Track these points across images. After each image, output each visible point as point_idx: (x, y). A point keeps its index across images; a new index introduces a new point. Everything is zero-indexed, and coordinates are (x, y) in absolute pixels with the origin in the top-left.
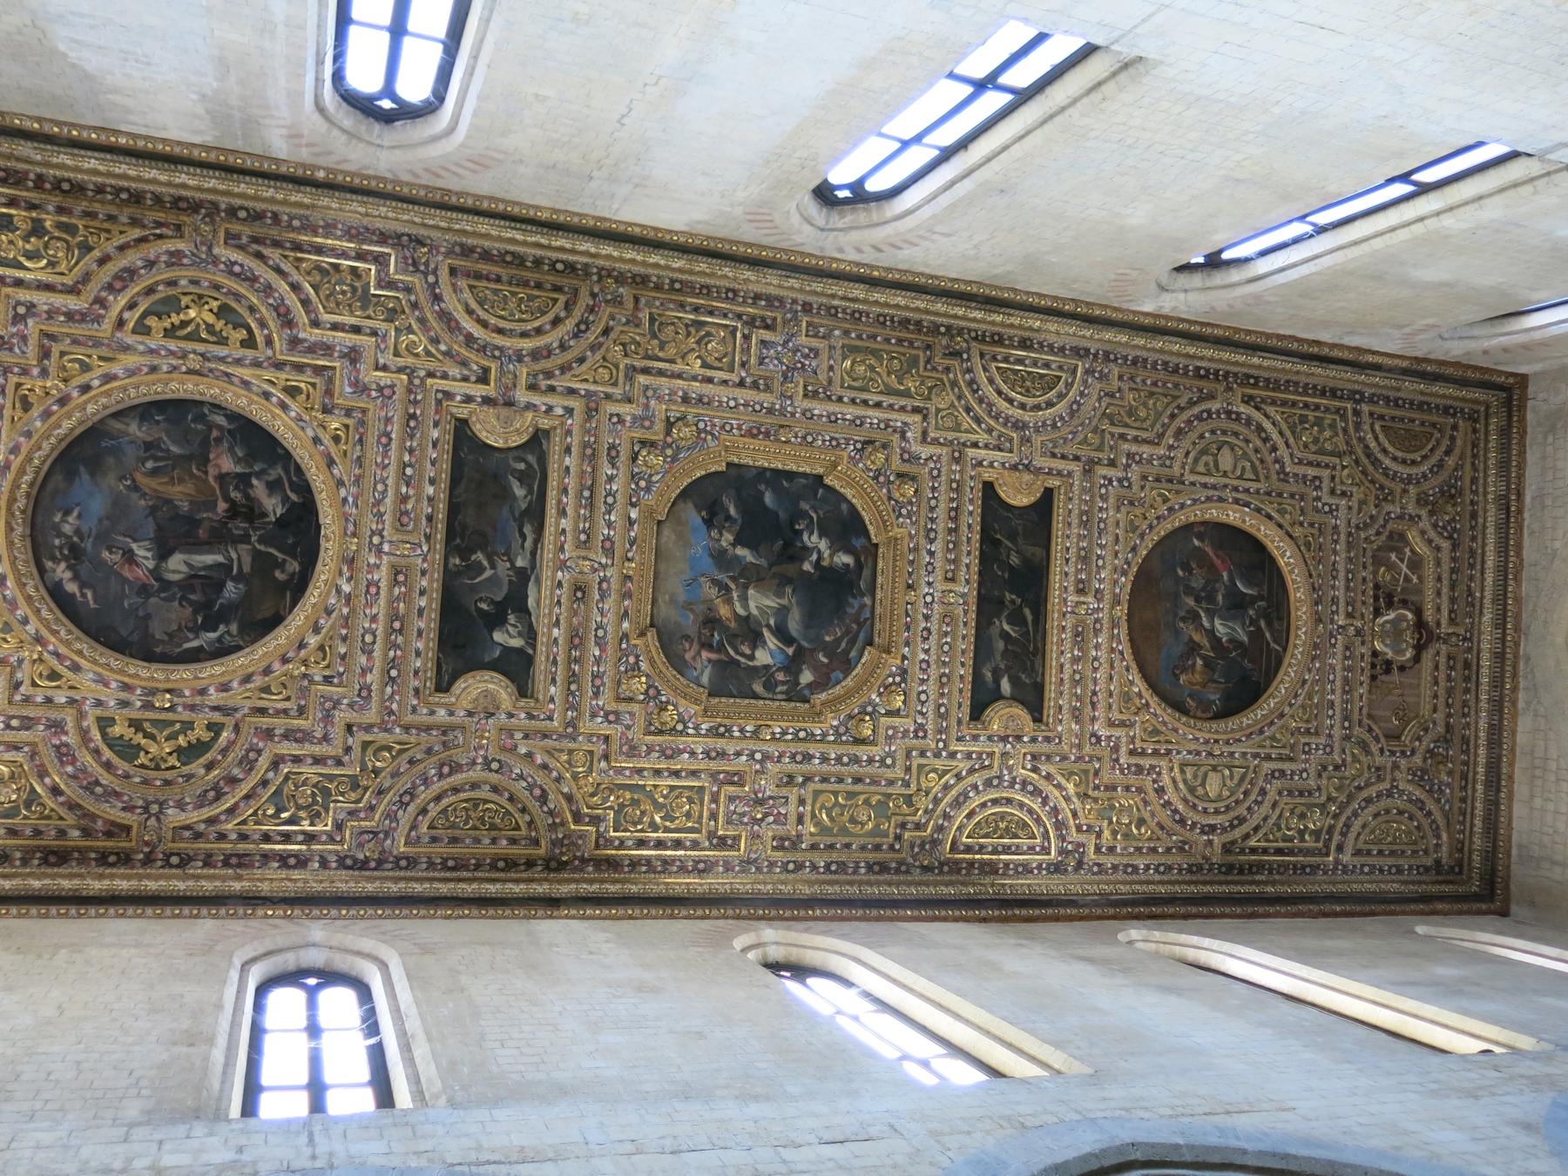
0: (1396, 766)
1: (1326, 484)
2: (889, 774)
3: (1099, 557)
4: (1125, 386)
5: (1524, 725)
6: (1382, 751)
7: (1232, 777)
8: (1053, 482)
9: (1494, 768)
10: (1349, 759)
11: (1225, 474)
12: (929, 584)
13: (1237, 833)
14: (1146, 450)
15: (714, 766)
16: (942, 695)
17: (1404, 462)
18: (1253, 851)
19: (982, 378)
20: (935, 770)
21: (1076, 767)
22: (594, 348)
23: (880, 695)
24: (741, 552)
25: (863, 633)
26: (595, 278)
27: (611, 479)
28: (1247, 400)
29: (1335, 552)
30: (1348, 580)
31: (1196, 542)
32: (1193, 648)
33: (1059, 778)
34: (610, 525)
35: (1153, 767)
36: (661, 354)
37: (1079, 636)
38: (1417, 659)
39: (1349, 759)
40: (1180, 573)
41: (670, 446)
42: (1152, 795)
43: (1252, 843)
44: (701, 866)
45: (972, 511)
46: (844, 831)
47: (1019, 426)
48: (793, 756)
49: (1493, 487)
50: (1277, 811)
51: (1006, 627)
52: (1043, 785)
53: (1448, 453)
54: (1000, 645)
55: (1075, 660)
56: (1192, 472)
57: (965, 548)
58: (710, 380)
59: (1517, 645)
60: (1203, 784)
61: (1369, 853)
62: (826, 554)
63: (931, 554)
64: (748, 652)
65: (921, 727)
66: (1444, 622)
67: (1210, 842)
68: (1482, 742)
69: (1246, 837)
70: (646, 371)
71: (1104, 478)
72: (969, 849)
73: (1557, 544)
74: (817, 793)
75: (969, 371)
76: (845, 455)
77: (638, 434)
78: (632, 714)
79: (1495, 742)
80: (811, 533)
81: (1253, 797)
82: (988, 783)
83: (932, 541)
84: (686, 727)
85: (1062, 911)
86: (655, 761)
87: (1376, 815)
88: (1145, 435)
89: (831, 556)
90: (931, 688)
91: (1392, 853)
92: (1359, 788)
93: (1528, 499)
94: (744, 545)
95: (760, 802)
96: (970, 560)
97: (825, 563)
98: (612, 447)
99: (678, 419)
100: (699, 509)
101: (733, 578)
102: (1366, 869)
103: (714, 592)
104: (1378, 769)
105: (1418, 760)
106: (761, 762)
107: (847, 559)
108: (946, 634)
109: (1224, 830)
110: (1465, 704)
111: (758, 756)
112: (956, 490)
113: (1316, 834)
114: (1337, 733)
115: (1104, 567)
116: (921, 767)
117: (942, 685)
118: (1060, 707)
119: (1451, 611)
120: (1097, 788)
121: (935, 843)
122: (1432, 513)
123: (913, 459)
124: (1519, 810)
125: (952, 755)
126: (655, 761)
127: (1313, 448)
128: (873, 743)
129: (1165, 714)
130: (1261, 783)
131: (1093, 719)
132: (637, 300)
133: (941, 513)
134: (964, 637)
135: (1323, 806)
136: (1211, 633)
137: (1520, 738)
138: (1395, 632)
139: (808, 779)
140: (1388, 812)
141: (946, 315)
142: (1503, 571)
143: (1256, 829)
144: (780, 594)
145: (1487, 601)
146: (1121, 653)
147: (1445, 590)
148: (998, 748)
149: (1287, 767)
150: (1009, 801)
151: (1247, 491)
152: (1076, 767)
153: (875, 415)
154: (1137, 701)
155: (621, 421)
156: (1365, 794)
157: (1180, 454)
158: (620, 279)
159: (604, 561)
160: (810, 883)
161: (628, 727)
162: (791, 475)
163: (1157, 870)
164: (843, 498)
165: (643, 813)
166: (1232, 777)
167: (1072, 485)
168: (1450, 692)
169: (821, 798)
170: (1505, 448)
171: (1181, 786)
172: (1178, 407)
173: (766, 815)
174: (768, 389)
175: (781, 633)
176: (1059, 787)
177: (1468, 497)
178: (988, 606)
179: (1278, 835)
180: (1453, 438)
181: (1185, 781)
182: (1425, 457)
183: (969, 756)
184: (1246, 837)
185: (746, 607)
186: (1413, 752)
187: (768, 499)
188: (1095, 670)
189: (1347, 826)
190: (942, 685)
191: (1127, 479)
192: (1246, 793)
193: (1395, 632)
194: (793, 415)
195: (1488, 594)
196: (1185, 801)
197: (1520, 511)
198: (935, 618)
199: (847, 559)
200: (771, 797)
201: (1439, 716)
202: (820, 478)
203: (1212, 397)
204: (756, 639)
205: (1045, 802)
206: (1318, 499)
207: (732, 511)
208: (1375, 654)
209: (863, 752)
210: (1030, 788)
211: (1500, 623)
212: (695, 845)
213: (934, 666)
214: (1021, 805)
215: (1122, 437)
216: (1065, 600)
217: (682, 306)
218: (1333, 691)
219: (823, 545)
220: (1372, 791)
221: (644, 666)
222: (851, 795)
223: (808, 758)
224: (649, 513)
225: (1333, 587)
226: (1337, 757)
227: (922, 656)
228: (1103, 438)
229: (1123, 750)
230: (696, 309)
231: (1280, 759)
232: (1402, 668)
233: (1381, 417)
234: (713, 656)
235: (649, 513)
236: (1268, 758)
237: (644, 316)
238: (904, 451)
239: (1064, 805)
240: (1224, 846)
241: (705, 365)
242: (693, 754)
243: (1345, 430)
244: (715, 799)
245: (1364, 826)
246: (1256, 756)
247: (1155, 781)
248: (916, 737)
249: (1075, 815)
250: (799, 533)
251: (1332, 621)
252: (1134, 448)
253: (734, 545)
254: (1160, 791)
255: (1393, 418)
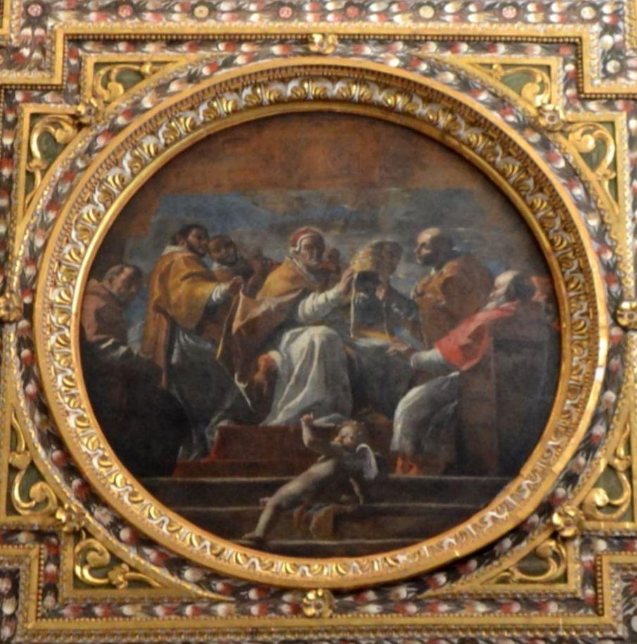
32: (249, 273)
40: (426, 236)
136: (287, 319)
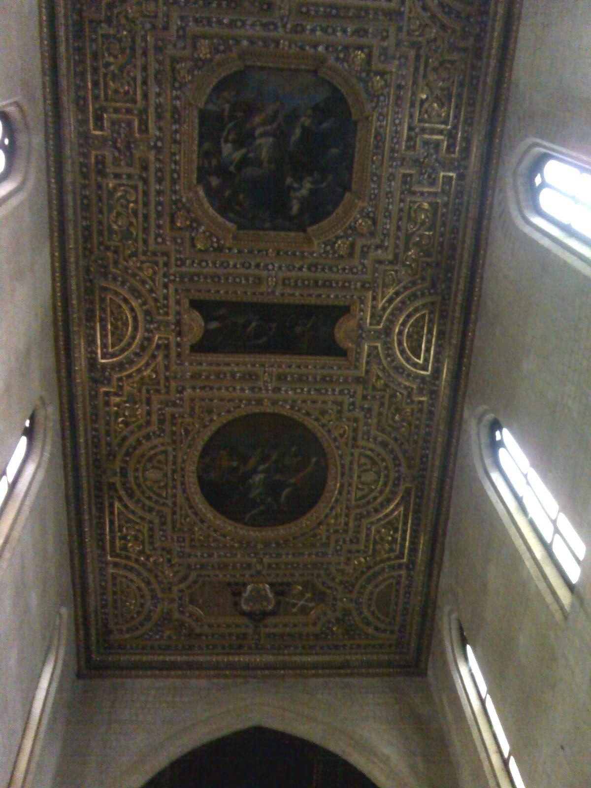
0: (172, 601)
1: (354, 547)
2: (151, 241)
3: (302, 390)
4: (415, 407)
5: (204, 683)
6: (181, 591)
7: (160, 488)
8: (352, 356)
9: (174, 666)
10: (175, 569)
11: (359, 477)
12: (280, 268)
13: (122, 493)
14: (373, 421)
15: (151, 110)
16: (206, 278)
17: (370, 599)
18: (111, 505)
19: (418, 303)
20: (155, 273)
21: (162, 377)
22: (433, 16)
23: (204, 232)
24: (298, 131)
25: (247, 222)
26: (480, 19)
27: (344, 31)
28: (408, 492)
29: (310, 555)
30: (292, 564)
31: (314, 460)
33: (153, 365)
34: (313, 31)
35: (163, 431)
36: (429, 69)
37: (251, 377)
38: (243, 613)
39: (175, 569)
40: (293, 449)
41: (368, 75)
42: (144, 431)
43: (117, 504)
44: (82, 102)
45: (331, 297)
46: (110, 210)
47: (388, 331)
48: (160, 170)
49: (355, 658)
50: (138, 521)
51: (254, 324)
52: (149, 352)
53: (377, 629)
54: (241, 320)
55: (233, 375)
56: (361, 454)
57: (305, 292)
58: (412, 105)
59: (254, 677)
60: (154, 467)
61: (114, 585)
62: (298, 194)
63: (301, 269)
64: (231, 137)
65: (183, 263)
66: (267, 630)
67: (115, 474)
68: (191, 658)
69: (120, 499)
70: (418, 57)
71: (355, 392)
72: (103, 300)
73: (319, 696)
74: (136, 188)
75: (423, 294)
76: (366, 204)
77: (376, 53)
79: (190, 666)
80: (311, 183)
81: (147, 502)
82: (147, 313)
83: (309, 269)
84: (176, 89)
85: (63, 366)
86: (153, 66)
87: (139, 589)
88: (384, 420)
89: (297, 198)
90: (210, 270)
91: (115, 601)
92: (156, 576)
93: (347, 680)
95: (128, 148)
96: (297, 297)
97: (292, 194)
98: (366, 32)
99: (386, 81)
102: (103, 584)
104: (170, 589)
105: (176, 615)
106: (155, 147)
107: (295, 208)
108: (247, 280)
109: (124, 484)
110: (215, 647)
112: (344, 287)
113: (124, 548)
114: (192, 560)
115: (296, 393)
116: (156, 263)
117: (212, 278)
118: (201, 364)
119: (274, 634)
120: (148, 391)
121: (105, 275)
122: (338, 619)
123: (364, 255)
124: (147, 682)
125: (166, 286)
126: (153, 66)
127: (377, 538)
128: (172, 229)
129: (200, 444)
130: (157, 508)
131: (194, 388)
132: (466, 50)
133: (328, 275)
134: (246, 293)
135: (142, 552)
136: (254, 471)
137: (194, 682)
138: (258, 596)
139: (146, 181)
140: (142, 596)
141: (459, 277)
142: (303, 667)
143: (126, 506)
145: (281, 658)
146: (239, 407)
147: (288, 629)
148: (171, 318)
149: (169, 526)
150: (136, 329)
151: (349, 493)
152: (162, 377)
153: (390, 226)
154: (207, 419)
155: (384, 39)
156: (153, 580)
157: (372, 446)
158: (479, 38)
159: (289, 26)
160: (73, 183)
161: (175, 45)
162: (350, 168)
163: (94, 437)
165: (116, 57)
166: (160, 488)
167: (348, 369)
168: (223, 636)
169: (132, 191)
170: (380, 664)
171: (152, 452)
172: (402, 444)
173: (119, 150)
174: (408, 148)
175: (244, 162)
176: (147, 365)
177: (349, 643)
178: (268, 312)
179: (123, 522)
180: (385, 631)
181: (155, 454)
182: (373, 613)
183: (166, 298)
184: (120, 499)
186: (182, 612)
187: (334, 151)
188: (227, 389)
189: (131, 569)
190: (212, 278)
191: (354, 409)
192: (150, 498)
193: (258, 596)
194: (391, 166)
195: (287, 658)
196: (143, 456)
197: (339, 675)
198: (257, 272)
199: (295, 208)
200: (131, 153)
201: (206, 629)
203: (409, 467)
204: (239, 143)
205: (137, 355)
206: (345, 542)
208: (245, 585)
209: (165, 221)
210: (146, 343)
211: (268, 667)
212: (96, 98)
213: (225, 271)
214: (133, 338)
215: (382, 404)
216: (273, 366)
217: (462, 85)
218: (219, 556)
219: (304, 192)
220: (155, 586)
222: (135, 213)
223: (160, 181)
224: (323, 61)
225: (288, 554)
226: (175, 560)
227: (231, 263)
228: (381, 390)
229: (175, 410)
230: (459, 95)
231: (174, 522)
232: (236, 604)
233: (398, 583)
234: (226, 113)
235: (323, 61)
236: (174, 513)
237: (455, 56)
238: (369, 247)
239: (135, 368)
240: (114, 484)
241: (422, 102)
243: (389, 559)
244: (129, 111)
245: (132, 581)
246: (175, 504)
247: (154, 433)
248: (177, 259)
249: (129, 376)
251: (265, 554)
252: (375, 413)
253: (303, 127)
254: (148, 437)
255: (397, 591)
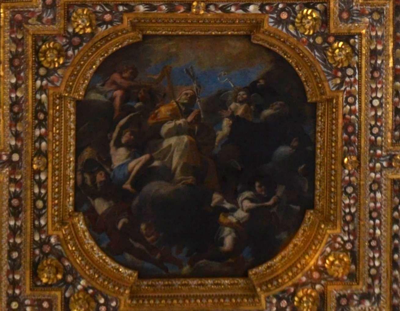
24: (226, 123)
25: (153, 266)
48: (16, 195)
62: (232, 219)
64: (124, 140)
78: (53, 21)
80: (251, 200)
84: (42, 78)
89: (230, 225)
94: (232, 127)
97: (222, 218)
100: (267, 76)
101: (197, 118)
103: (183, 99)
106: (10, 162)
111: (16, 157)
128: (34, 286)
144: (185, 169)
162: (310, 173)
164: (293, 232)
175: (146, 174)
185: (170, 134)
187: (284, 150)
202: (312, 205)
204: (135, 149)
207: (267, 112)
221: (102, 29)
242: (15, 87)
250: (250, 187)
253: (232, 116)
